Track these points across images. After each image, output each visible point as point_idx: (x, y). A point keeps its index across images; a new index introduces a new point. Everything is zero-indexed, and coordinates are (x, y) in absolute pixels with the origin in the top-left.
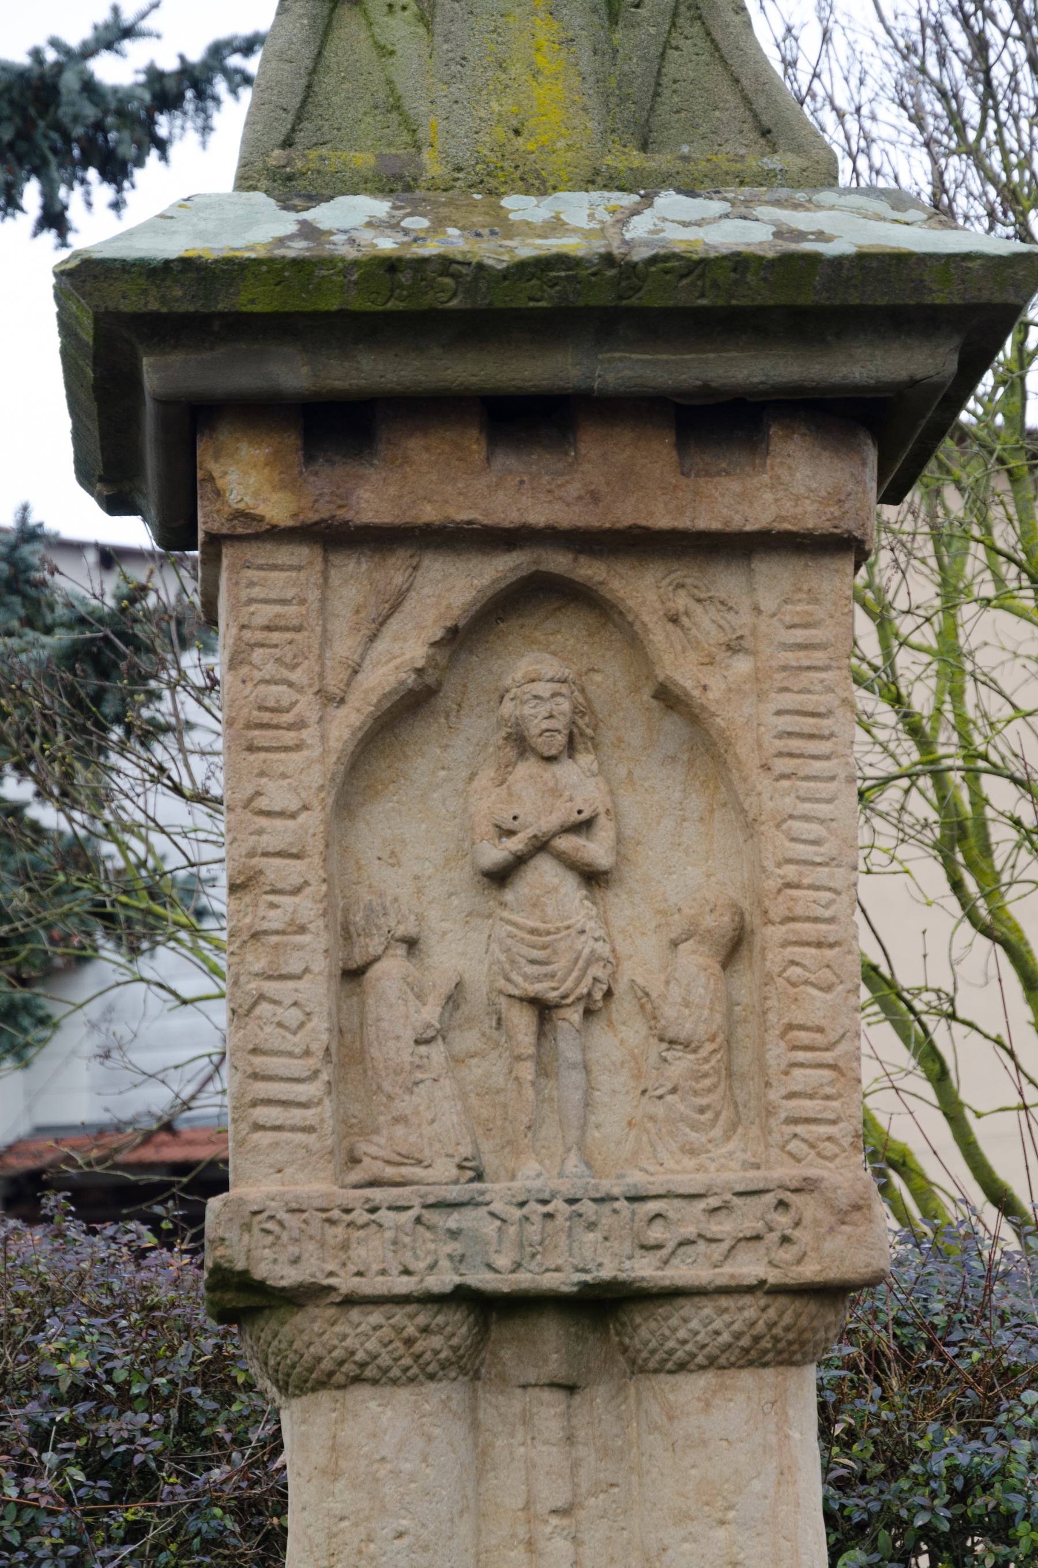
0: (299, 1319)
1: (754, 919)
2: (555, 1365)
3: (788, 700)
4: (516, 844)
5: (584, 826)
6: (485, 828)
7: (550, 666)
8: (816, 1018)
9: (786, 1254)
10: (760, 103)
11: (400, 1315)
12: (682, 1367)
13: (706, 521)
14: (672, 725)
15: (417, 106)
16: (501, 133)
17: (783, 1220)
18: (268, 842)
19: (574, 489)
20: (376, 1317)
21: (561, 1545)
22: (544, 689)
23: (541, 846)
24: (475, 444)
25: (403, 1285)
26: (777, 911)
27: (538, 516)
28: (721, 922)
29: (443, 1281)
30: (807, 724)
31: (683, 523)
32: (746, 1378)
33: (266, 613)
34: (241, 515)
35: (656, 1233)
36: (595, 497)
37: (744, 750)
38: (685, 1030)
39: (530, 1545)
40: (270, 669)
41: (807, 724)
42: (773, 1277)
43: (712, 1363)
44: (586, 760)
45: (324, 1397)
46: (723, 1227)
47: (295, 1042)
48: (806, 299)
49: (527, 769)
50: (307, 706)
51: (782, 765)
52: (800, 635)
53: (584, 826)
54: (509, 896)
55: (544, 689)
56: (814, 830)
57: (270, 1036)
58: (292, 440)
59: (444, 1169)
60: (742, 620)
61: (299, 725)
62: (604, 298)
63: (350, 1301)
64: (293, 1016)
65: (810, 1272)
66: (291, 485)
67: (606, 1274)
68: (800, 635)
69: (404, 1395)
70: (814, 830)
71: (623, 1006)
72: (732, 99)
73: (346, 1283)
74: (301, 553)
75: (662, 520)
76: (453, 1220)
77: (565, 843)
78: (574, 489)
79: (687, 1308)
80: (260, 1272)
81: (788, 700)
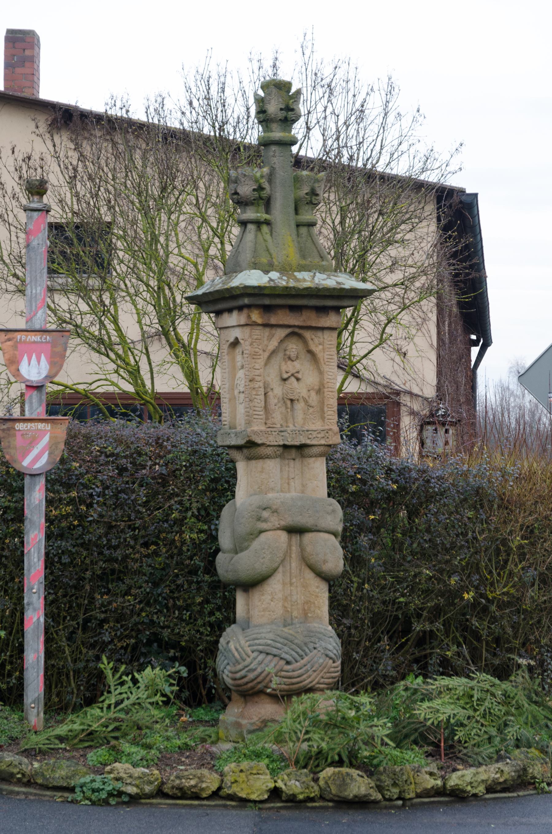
0: (259, 448)
1: (322, 387)
2: (293, 456)
3: (328, 353)
4: (289, 374)
5: (298, 372)
6: (284, 372)
7: (294, 347)
8: (331, 403)
9: (327, 440)
10: (321, 252)
11: (275, 448)
12: (311, 457)
13: (320, 325)
14: (309, 356)
15: (272, 251)
16: (285, 257)
17: (327, 435)
18: (256, 374)
19: (302, 319)
20: (271, 448)
21: (293, 483)
22: (294, 350)
23: (293, 375)
24: (287, 311)
25: (276, 444)
26: (326, 386)
27: (296, 323)
28: (316, 388)
29: (281, 443)
30: (330, 357)
31: (317, 325)
32: (319, 459)
33: (256, 337)
34: (254, 322)
35: (310, 436)
36: (304, 321)
37: (322, 361)
38: (313, 404)
39: (288, 484)
40: (256, 346)
41: (330, 357)
42: (326, 443)
43: (316, 456)
44: (298, 361)
45: (261, 460)
46: (319, 436)
47: (259, 405)
48: (343, 294)
49: (289, 362)
50: (261, 352)
51: (327, 363)
52: (330, 343)
53: (298, 372)
54: (286, 382)
55: (294, 350)
56: (331, 374)
57: (256, 404)
58: (262, 310)
59: (279, 426)
60: (322, 340)
61: (260, 355)
62: (315, 293)
63: (269, 446)
64: (259, 401)
65: (331, 443)
66: (262, 317)
67: (303, 442)
68: (330, 343)
69: (273, 460)
70: (331, 374)
71: (301, 400)
72: (315, 250)
73: (268, 443)
74: (261, 328)
75: (314, 325)
76: (283, 434)
77: (296, 375)
78: (302, 319)
79: (313, 448)
80: (256, 441)
81: (328, 353)
